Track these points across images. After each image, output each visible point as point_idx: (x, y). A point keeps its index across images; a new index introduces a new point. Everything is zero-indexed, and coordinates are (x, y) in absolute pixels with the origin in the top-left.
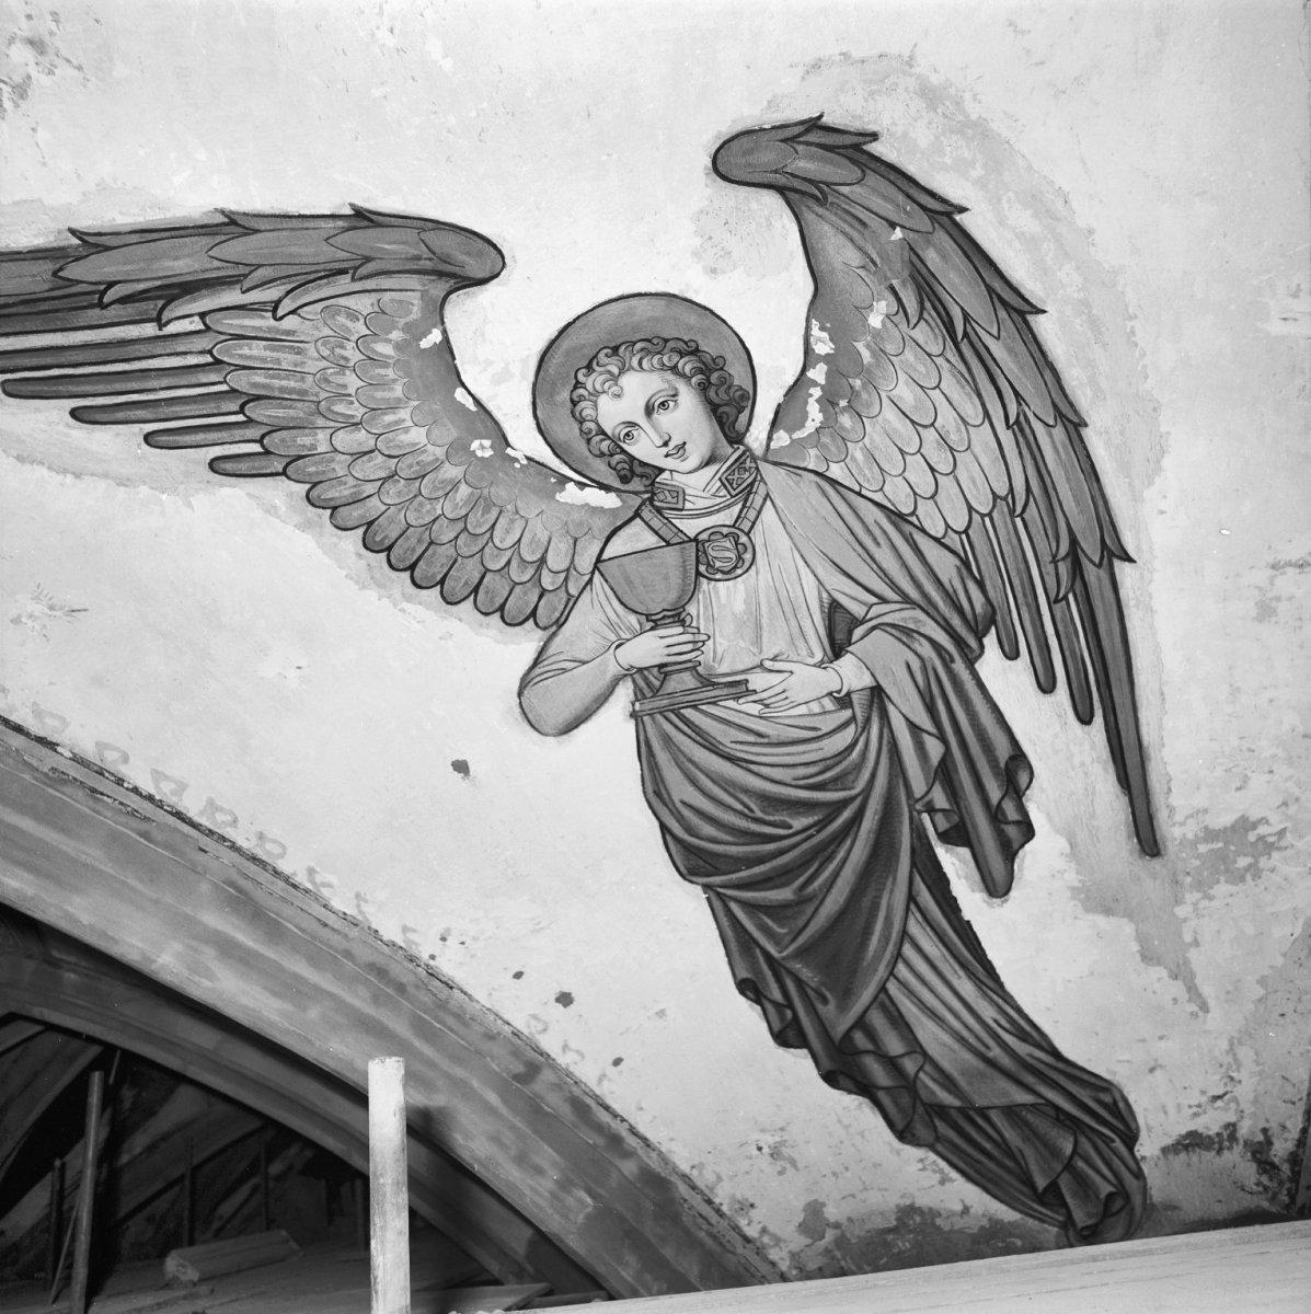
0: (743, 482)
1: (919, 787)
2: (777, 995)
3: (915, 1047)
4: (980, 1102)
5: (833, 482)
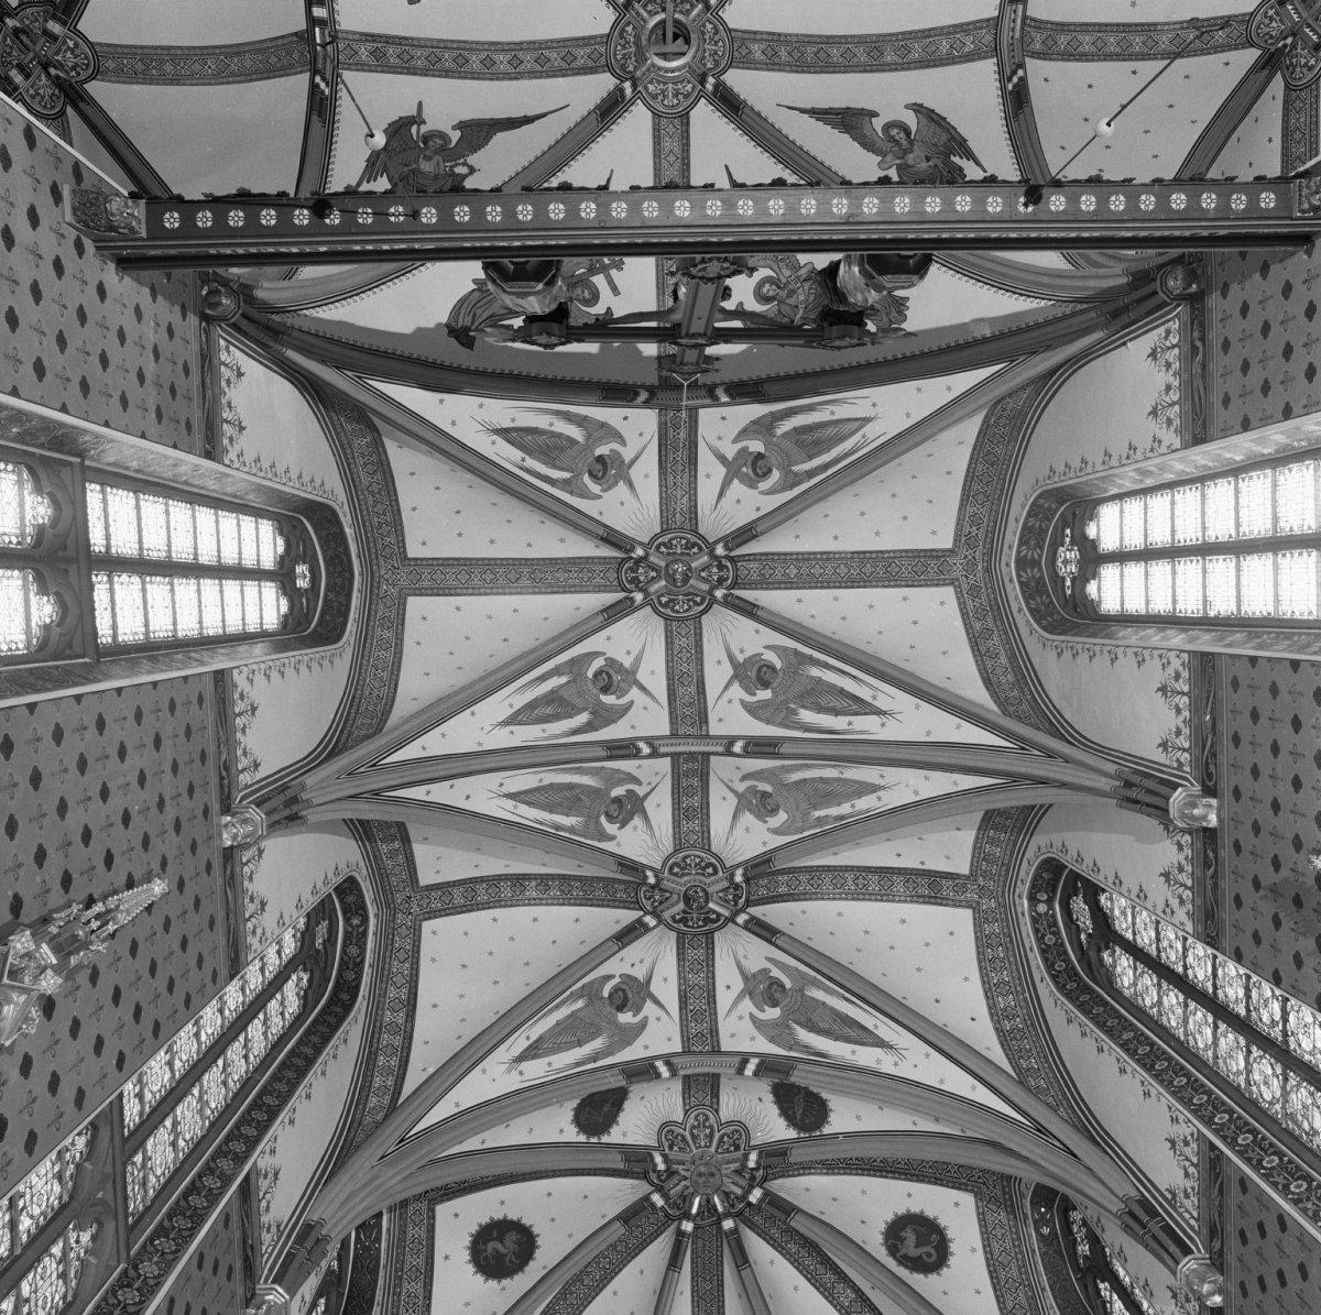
0: (911, 142)
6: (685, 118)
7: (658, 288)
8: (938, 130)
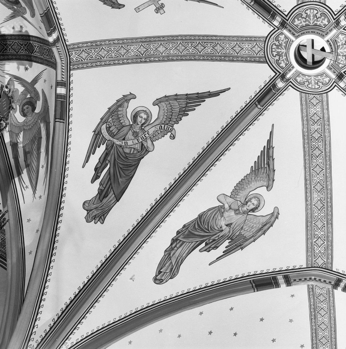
0: (246, 213)
1: (212, 238)
2: (183, 230)
3: (178, 248)
4: (172, 259)
5: (245, 221)
6: (265, 60)
7: (146, 38)
8: (254, 230)
